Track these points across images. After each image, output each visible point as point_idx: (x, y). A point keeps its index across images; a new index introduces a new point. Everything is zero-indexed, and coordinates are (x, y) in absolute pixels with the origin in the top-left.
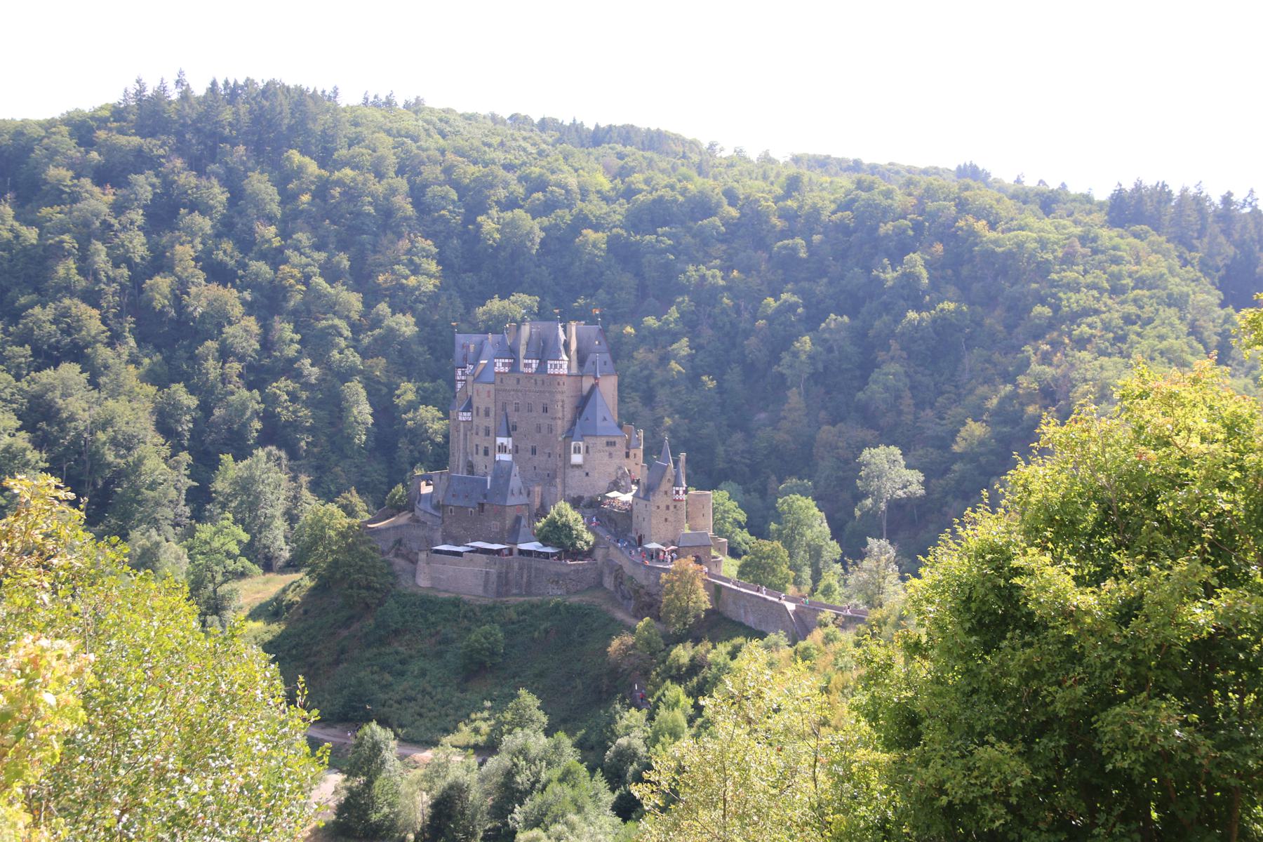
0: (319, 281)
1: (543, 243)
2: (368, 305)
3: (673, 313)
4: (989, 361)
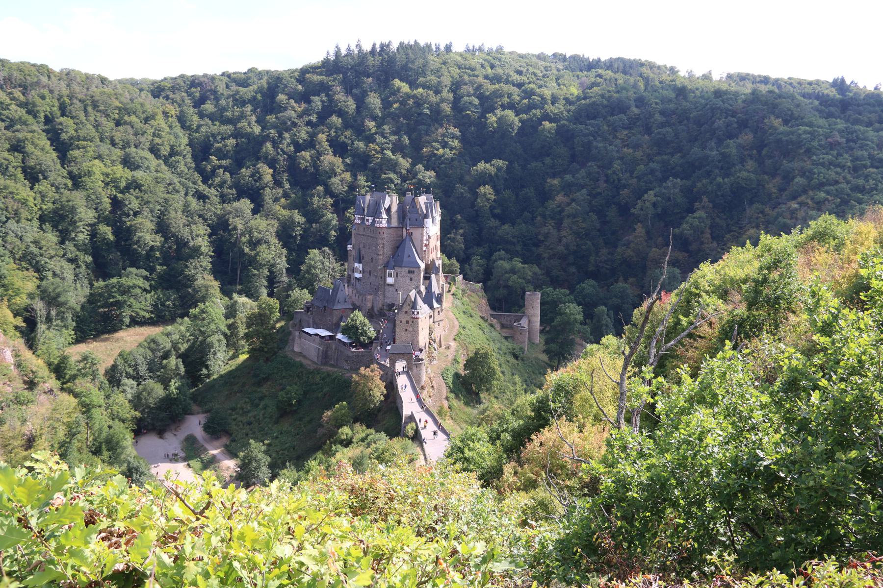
0: (389, 153)
1: (520, 129)
2: (413, 165)
3: (583, 172)
4: (762, 212)
